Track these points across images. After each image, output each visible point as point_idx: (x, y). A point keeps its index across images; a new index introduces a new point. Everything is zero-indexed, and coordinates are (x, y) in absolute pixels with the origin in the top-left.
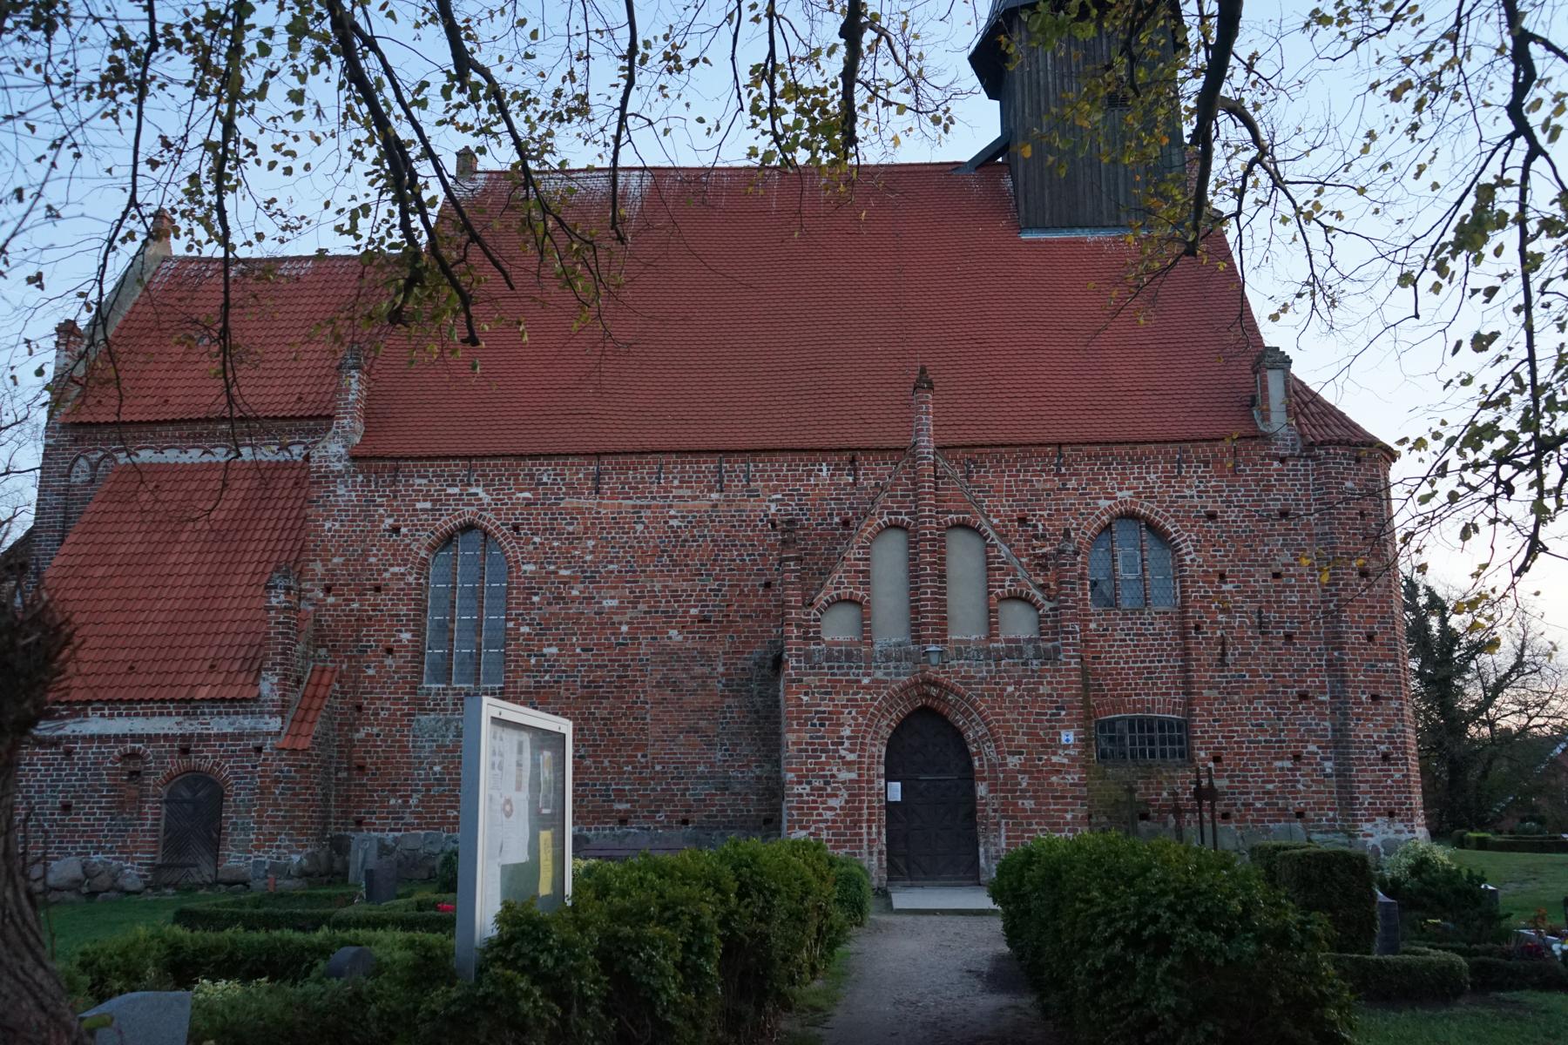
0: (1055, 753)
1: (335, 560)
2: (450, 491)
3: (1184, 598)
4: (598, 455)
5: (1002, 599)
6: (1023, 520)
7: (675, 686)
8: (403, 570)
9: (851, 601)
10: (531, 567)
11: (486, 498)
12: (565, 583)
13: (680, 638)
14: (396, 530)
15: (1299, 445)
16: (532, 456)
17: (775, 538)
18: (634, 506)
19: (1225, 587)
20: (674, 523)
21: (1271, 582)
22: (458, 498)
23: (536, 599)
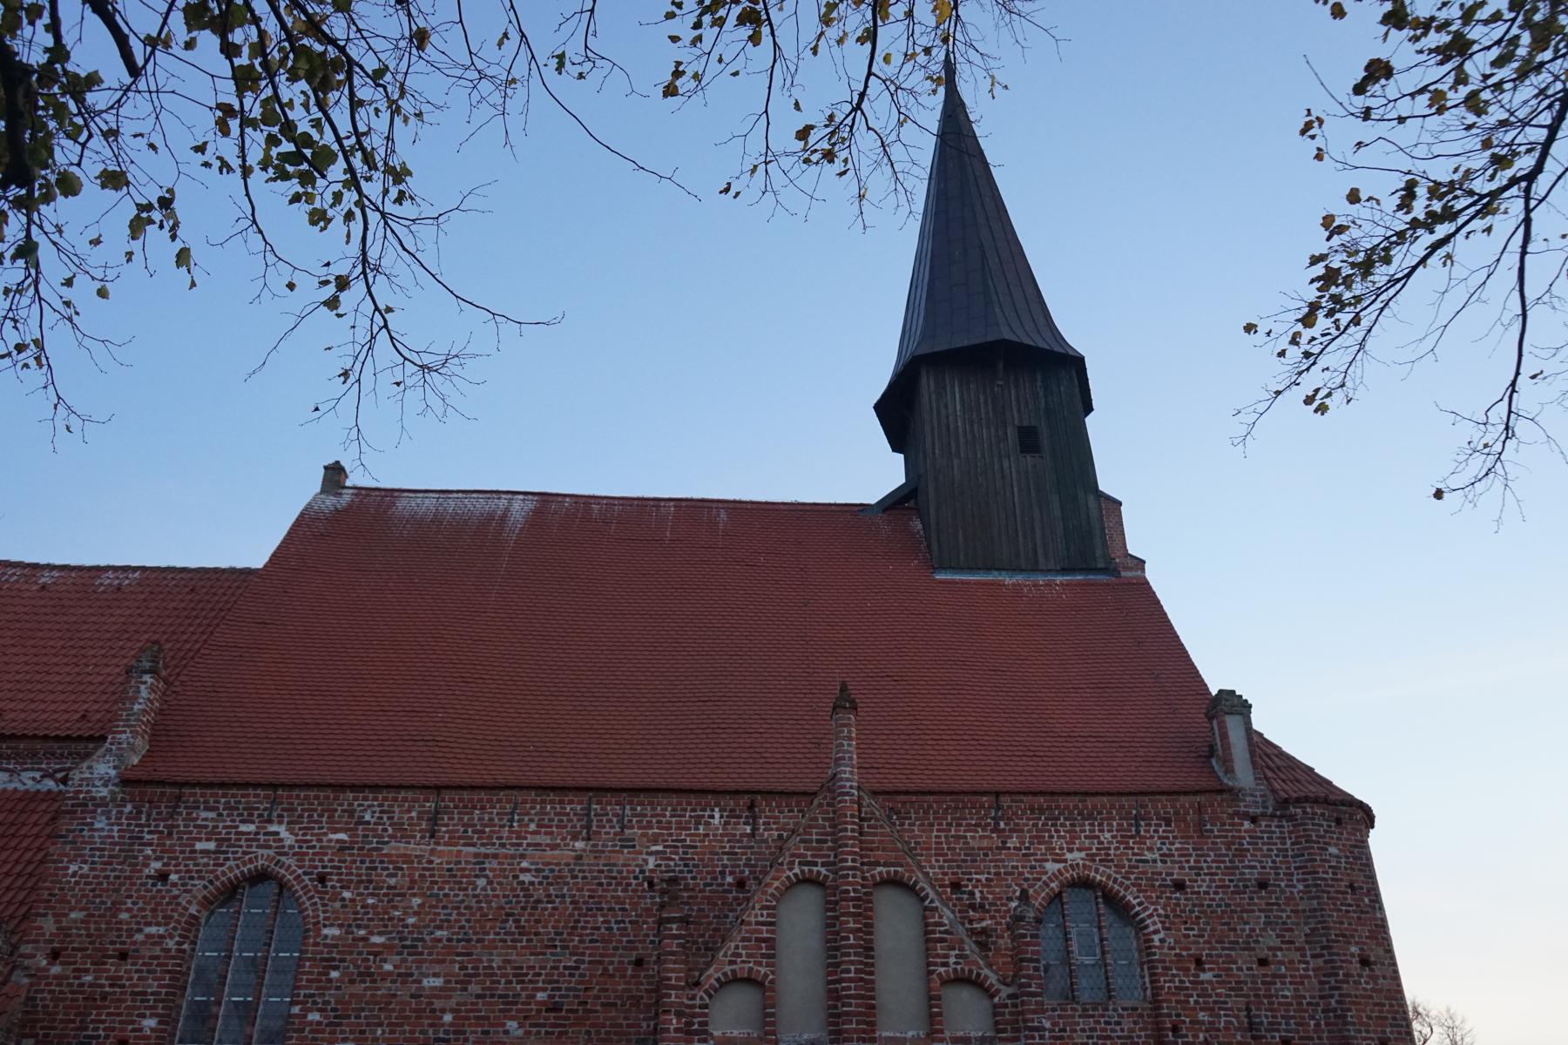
1: (73, 915)
2: (243, 828)
3: (1157, 991)
4: (438, 788)
5: (946, 982)
6: (956, 886)
8: (162, 930)
9: (750, 981)
10: (336, 932)
12: (376, 954)
13: (520, 1032)
14: (163, 877)
15: (1271, 803)
16: (354, 788)
17: (651, 900)
18: (476, 855)
19: (1205, 976)
21: (1259, 971)
22: (252, 838)
23: (334, 974)
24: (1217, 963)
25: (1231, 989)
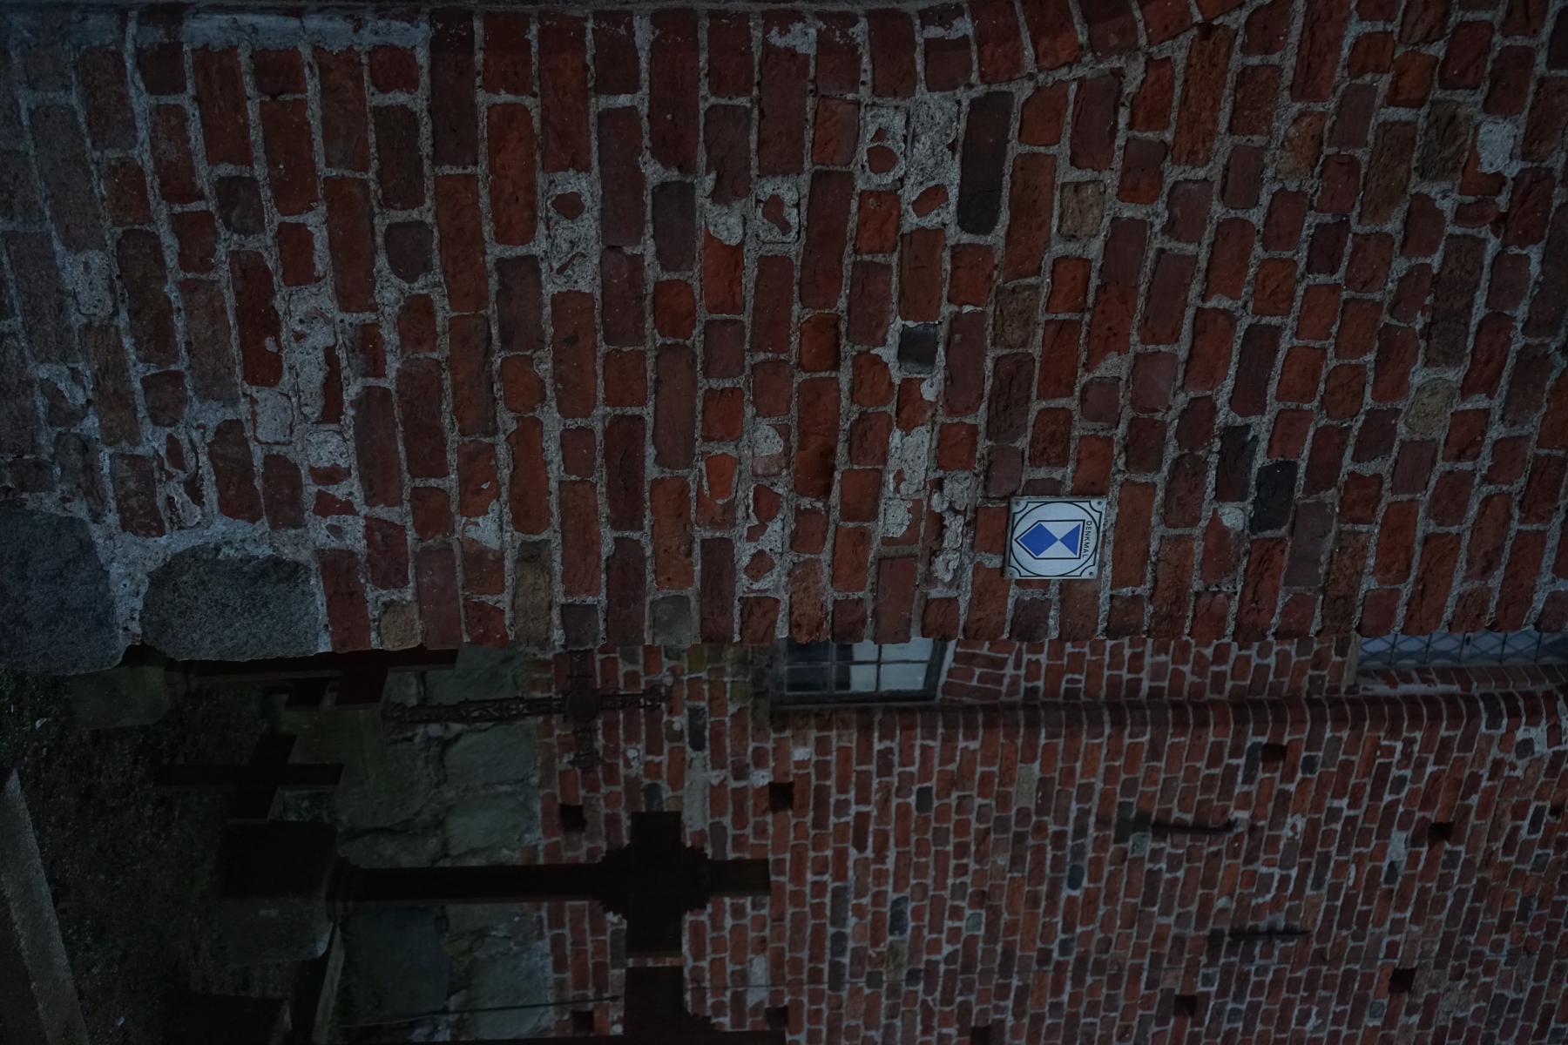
0: (950, 453)
24: (1427, 875)
25: (1350, 901)
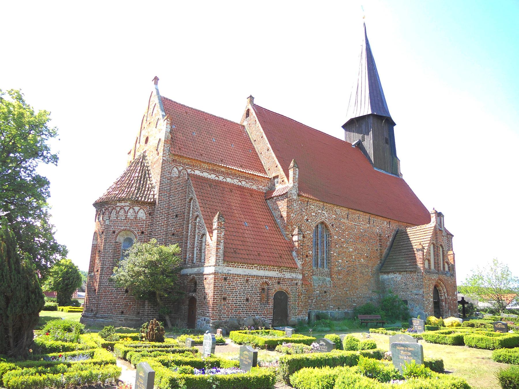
7: (363, 273)
11: (327, 216)
20: (361, 230)
